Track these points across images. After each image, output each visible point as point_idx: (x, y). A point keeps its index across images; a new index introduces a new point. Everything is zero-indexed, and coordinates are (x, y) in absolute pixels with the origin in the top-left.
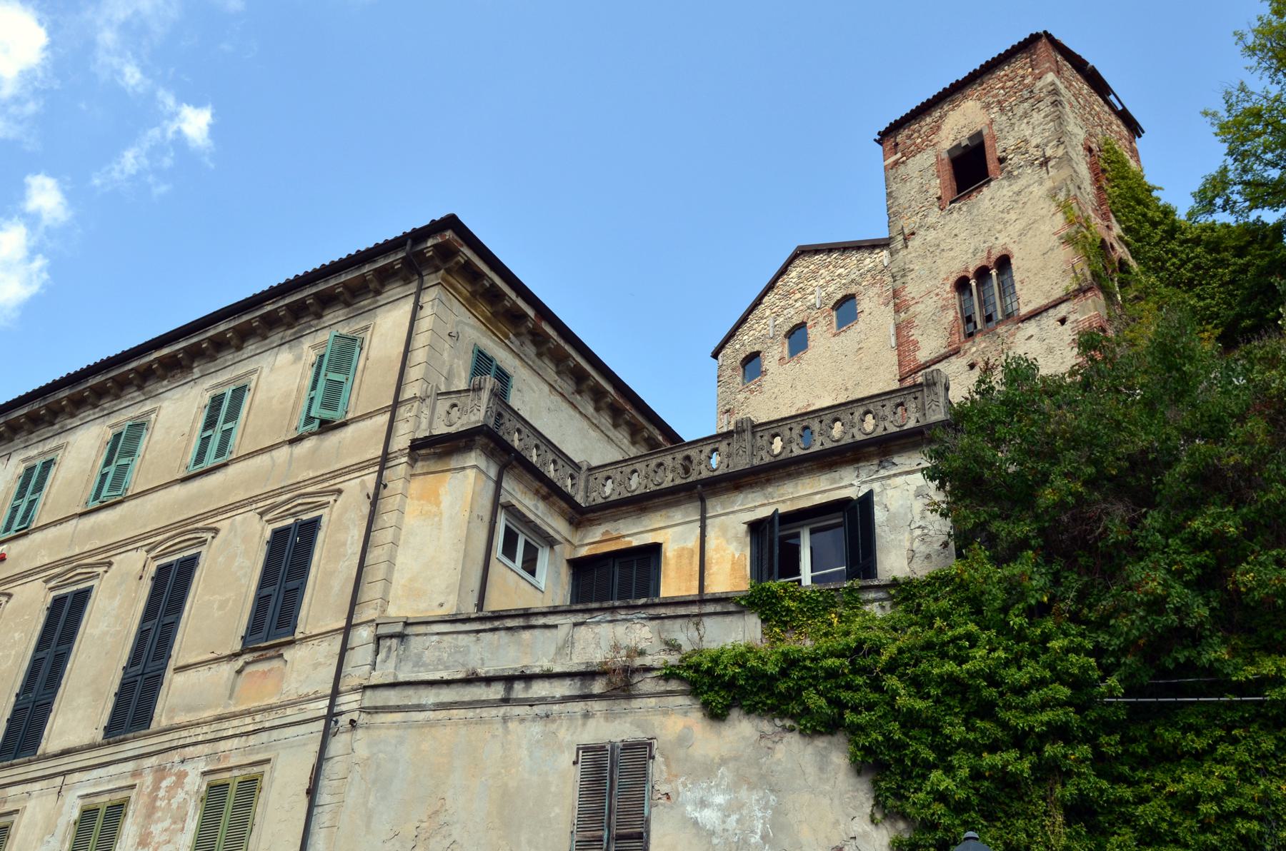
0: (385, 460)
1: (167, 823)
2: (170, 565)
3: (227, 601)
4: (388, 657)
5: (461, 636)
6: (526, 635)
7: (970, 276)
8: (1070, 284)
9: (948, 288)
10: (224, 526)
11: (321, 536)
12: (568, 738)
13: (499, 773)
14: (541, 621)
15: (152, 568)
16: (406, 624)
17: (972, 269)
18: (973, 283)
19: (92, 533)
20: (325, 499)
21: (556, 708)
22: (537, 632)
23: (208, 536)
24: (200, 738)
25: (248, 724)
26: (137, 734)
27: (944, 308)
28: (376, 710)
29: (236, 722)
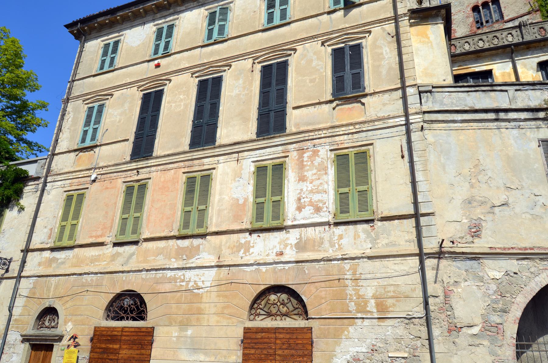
0: (396, 18)
1: (315, 171)
2: (207, 80)
3: (315, 79)
4: (427, 100)
5: (460, 93)
6: (492, 94)
7: (480, 5)
8: (527, 9)
9: (469, 10)
10: (300, 48)
11: (364, 51)
12: (532, 136)
13: (503, 150)
14: (499, 88)
15: (258, 67)
16: (433, 87)
17: (480, 3)
18: (481, 8)
19: (212, 54)
20: (289, 52)
21: (521, 123)
22: (497, 93)
23: (167, 82)
24: (323, 136)
25: (352, 129)
26: (281, 134)
27: (467, 17)
28: (432, 122)
29: (343, 129)
